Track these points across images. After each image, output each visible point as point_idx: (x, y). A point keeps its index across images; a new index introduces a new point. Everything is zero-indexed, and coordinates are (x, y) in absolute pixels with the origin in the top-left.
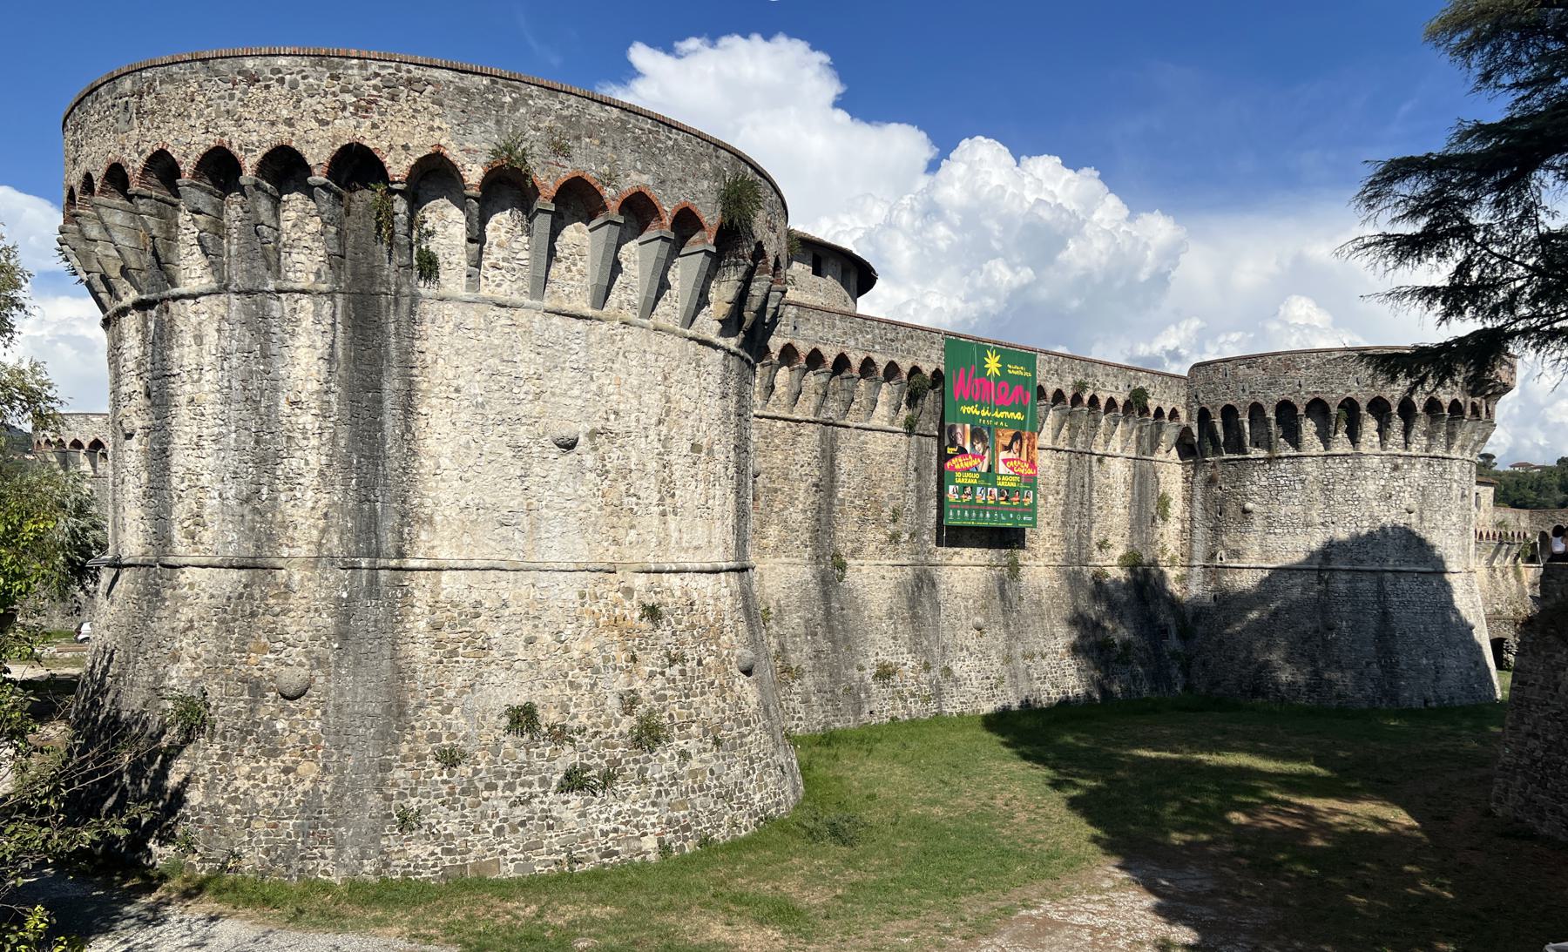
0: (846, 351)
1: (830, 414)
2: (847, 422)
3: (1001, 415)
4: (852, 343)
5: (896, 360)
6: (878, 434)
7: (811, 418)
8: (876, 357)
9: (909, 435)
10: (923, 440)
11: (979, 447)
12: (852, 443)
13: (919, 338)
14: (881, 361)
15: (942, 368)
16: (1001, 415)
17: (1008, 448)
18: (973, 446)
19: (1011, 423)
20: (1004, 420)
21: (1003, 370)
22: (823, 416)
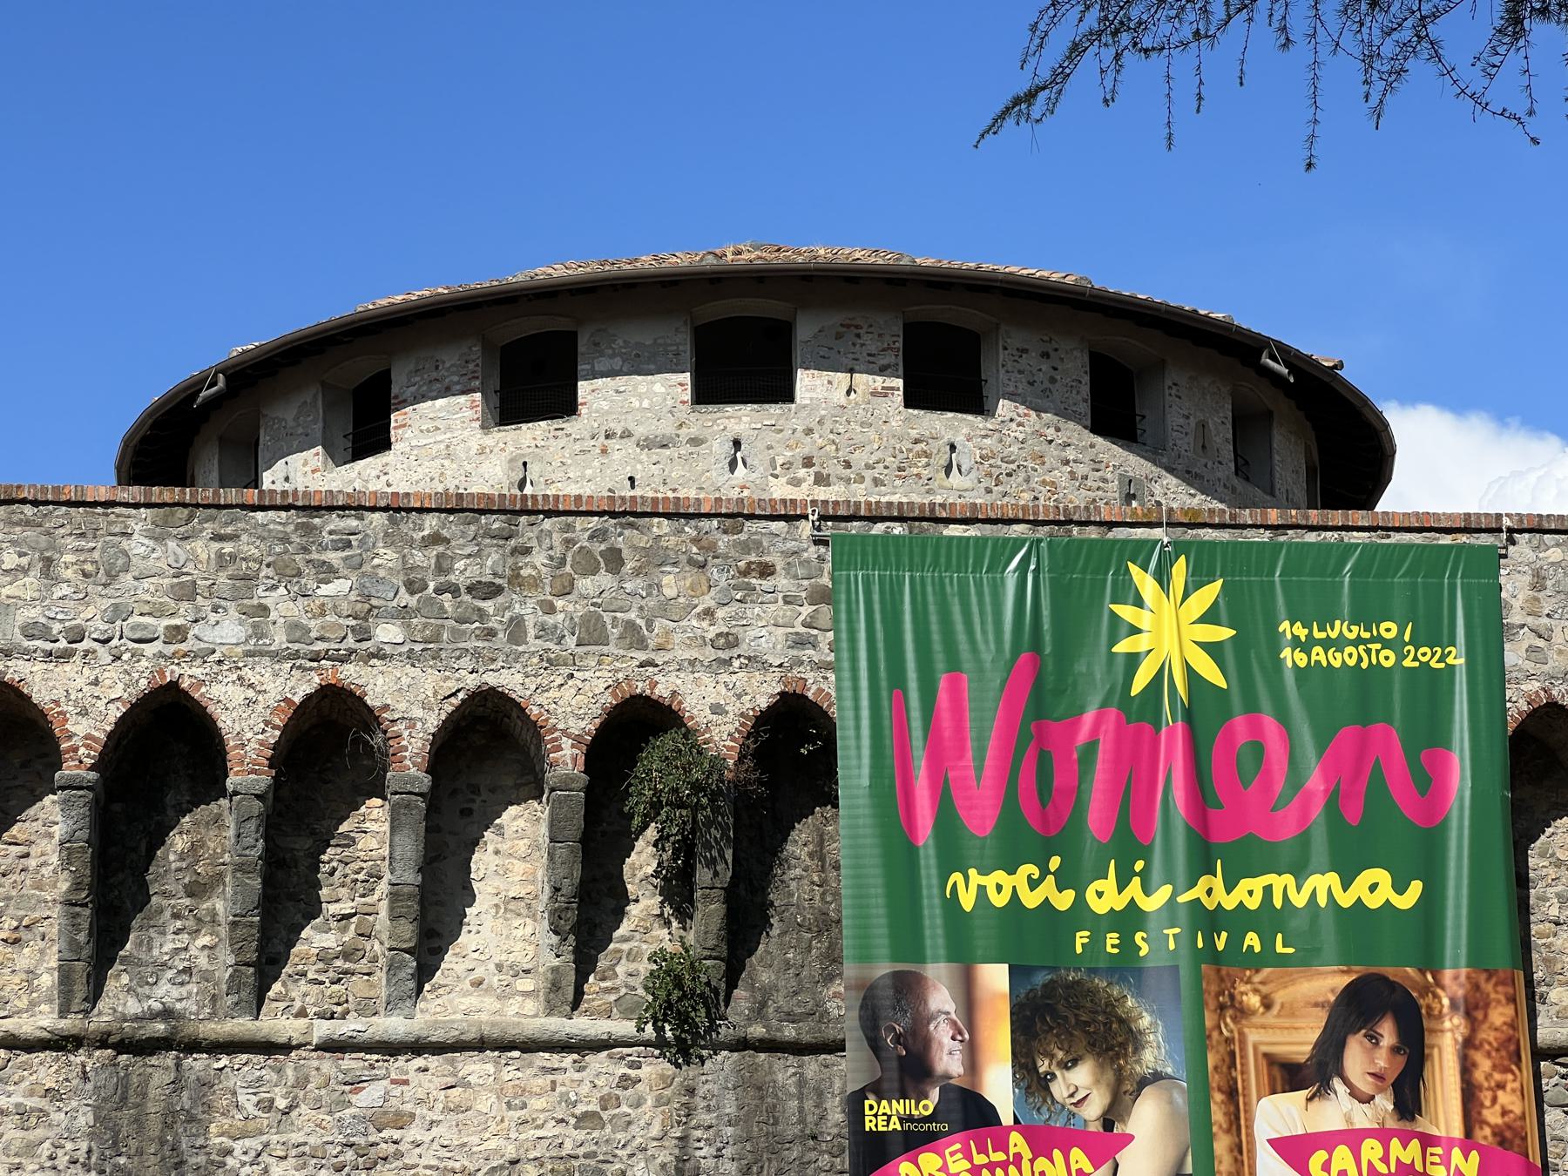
0: (188, 674)
1: (166, 992)
2: (275, 1023)
3: (1249, 893)
4: (228, 631)
5: (509, 680)
6: (476, 1067)
7: (45, 1020)
8: (378, 685)
9: (683, 1050)
10: (784, 1071)
11: (1080, 1085)
12: (308, 1127)
13: (655, 559)
14: (411, 700)
15: (819, 686)
16: (1249, 893)
17: (1309, 1075)
18: (1031, 1082)
19: (1312, 934)
20: (1269, 918)
21: (1248, 651)
22: (121, 1001)
